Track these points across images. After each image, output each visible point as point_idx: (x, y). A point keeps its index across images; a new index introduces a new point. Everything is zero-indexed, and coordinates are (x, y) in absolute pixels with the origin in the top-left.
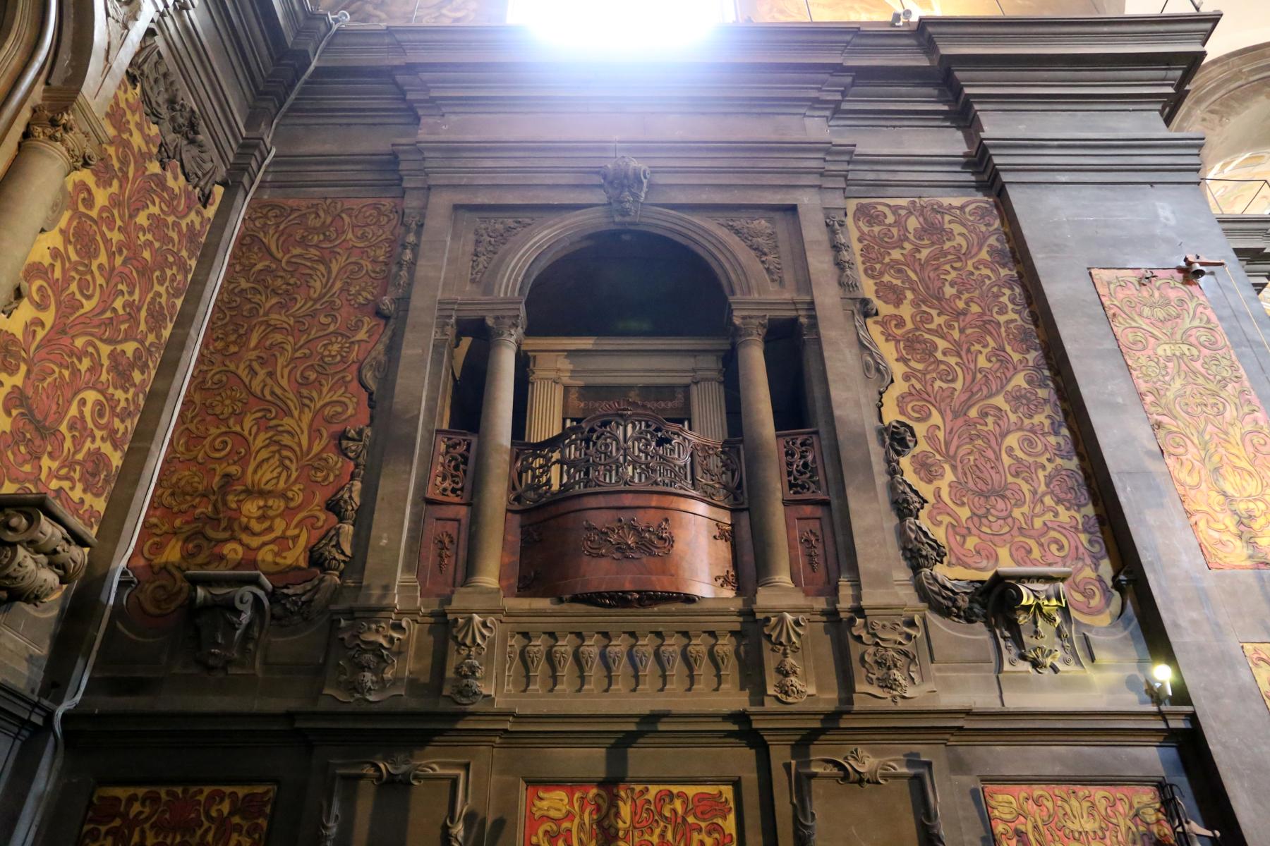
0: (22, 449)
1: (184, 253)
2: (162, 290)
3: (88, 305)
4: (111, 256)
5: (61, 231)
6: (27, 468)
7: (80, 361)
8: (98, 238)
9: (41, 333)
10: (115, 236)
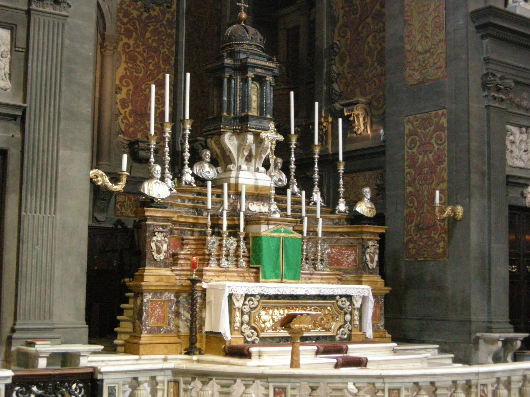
0: (139, 123)
1: (169, 31)
2: (165, 50)
3: (141, 75)
4: (142, 55)
5: (124, 62)
6: (142, 127)
7: (145, 91)
8: (136, 54)
9: (131, 92)
10: (141, 49)
